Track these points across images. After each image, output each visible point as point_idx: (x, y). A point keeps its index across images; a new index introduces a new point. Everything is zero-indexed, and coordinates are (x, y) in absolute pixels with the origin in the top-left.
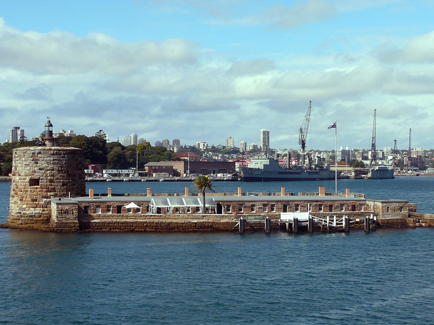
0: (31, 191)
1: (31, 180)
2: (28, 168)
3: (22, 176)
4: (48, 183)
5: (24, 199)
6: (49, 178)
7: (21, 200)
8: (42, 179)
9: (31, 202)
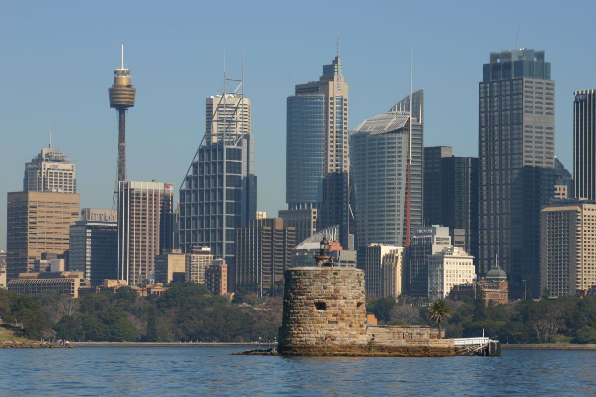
5: (354, 325)
7: (350, 326)
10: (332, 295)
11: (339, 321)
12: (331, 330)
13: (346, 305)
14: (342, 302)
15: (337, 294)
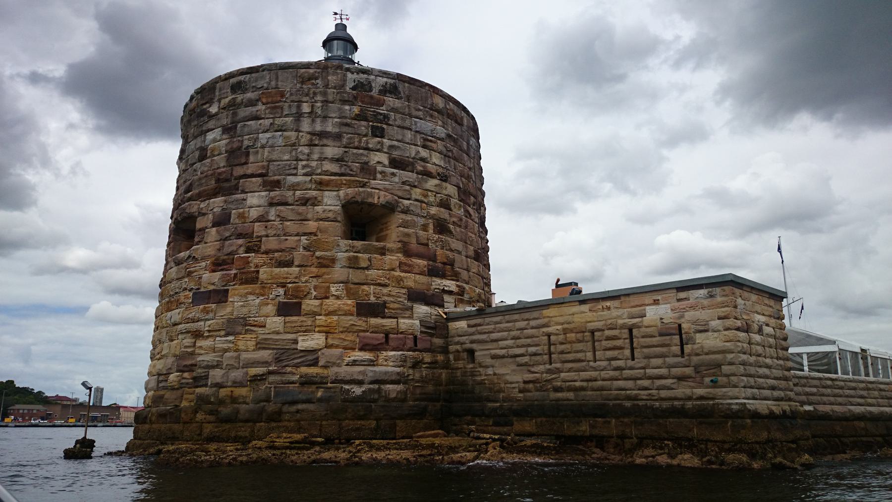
0: (353, 264)
2: (332, 151)
3: (294, 187)
5: (310, 304)
6: (434, 210)
8: (406, 211)
9: (360, 323)
10: (218, 181)
11: (236, 293)
12: (198, 335)
13: (273, 213)
14: (256, 200)
15: (239, 171)
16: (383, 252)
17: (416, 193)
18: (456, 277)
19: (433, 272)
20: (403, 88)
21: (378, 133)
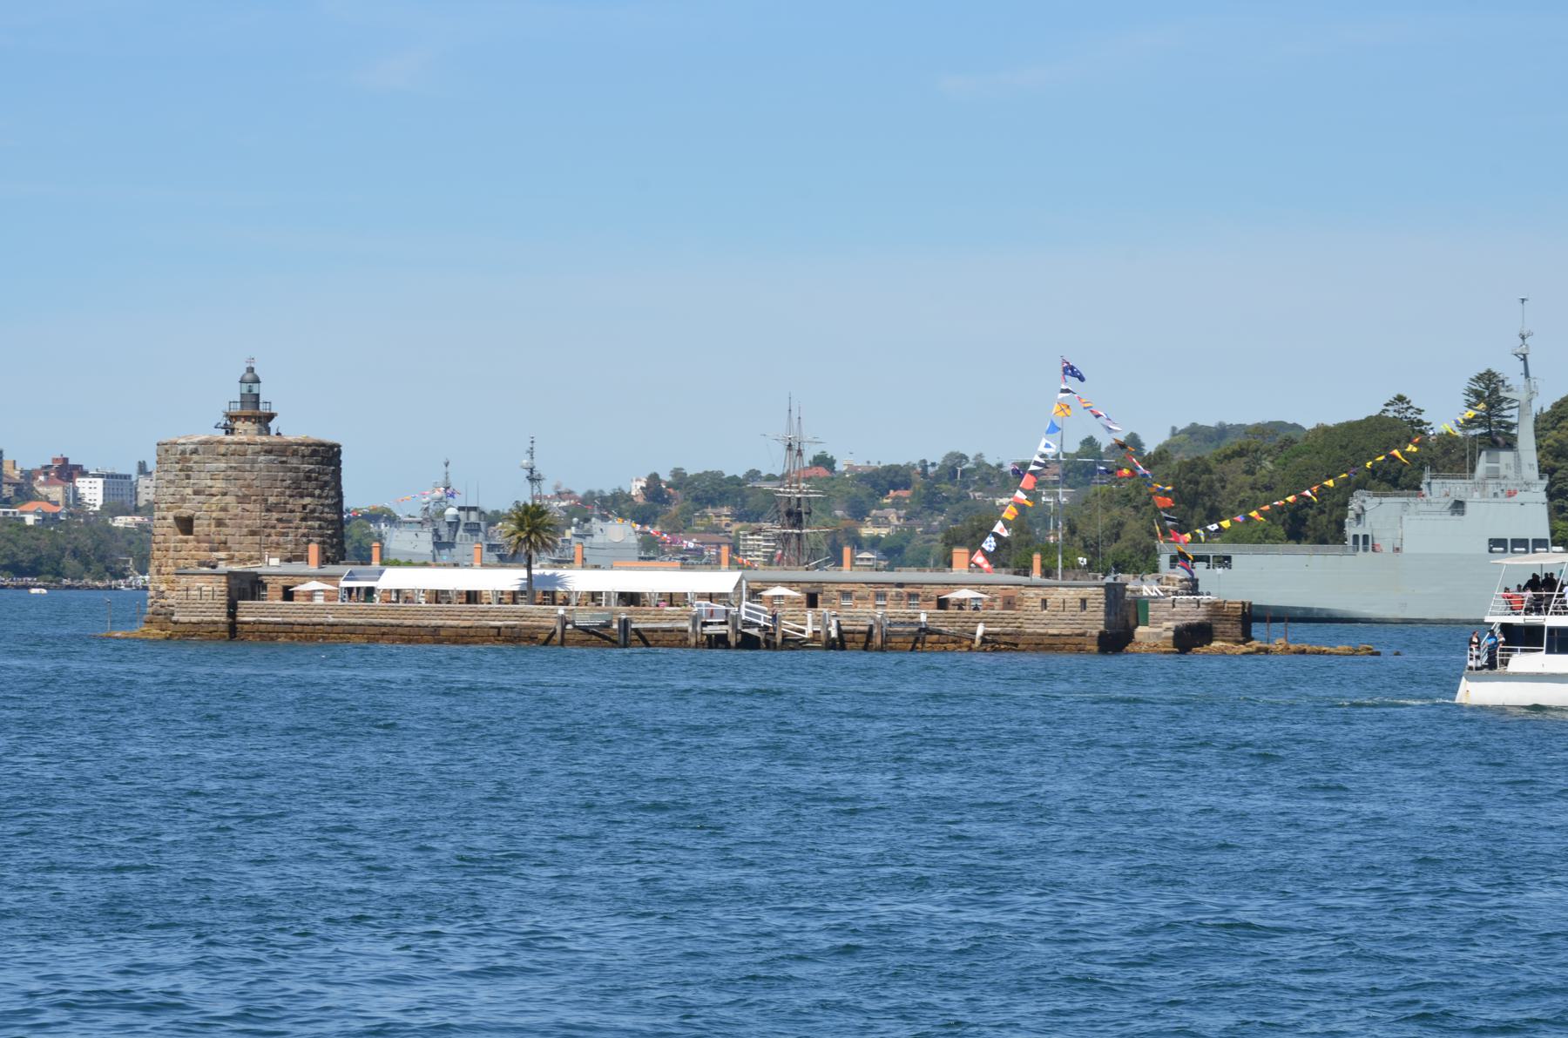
1: (176, 518)
4: (213, 529)
16: (186, 542)
17: (205, 507)
18: (229, 549)
19: (212, 550)
20: (201, 449)
21: (188, 477)
